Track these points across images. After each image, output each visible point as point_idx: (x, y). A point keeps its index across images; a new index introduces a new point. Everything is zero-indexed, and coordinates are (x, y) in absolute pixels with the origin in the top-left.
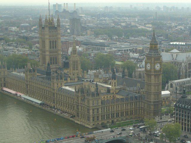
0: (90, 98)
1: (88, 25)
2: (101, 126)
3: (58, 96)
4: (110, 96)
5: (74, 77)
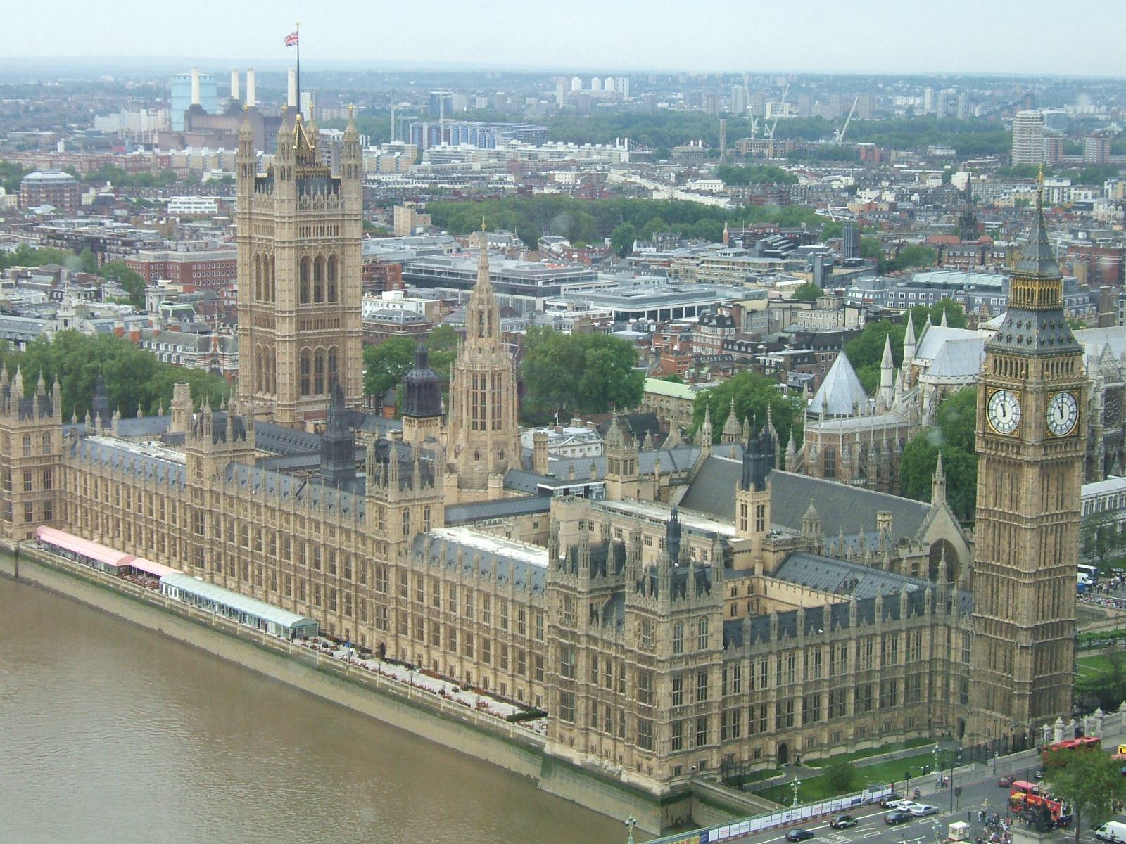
0: (660, 604)
1: (379, 182)
2: (719, 779)
3: (411, 585)
4: (734, 591)
5: (477, 466)
